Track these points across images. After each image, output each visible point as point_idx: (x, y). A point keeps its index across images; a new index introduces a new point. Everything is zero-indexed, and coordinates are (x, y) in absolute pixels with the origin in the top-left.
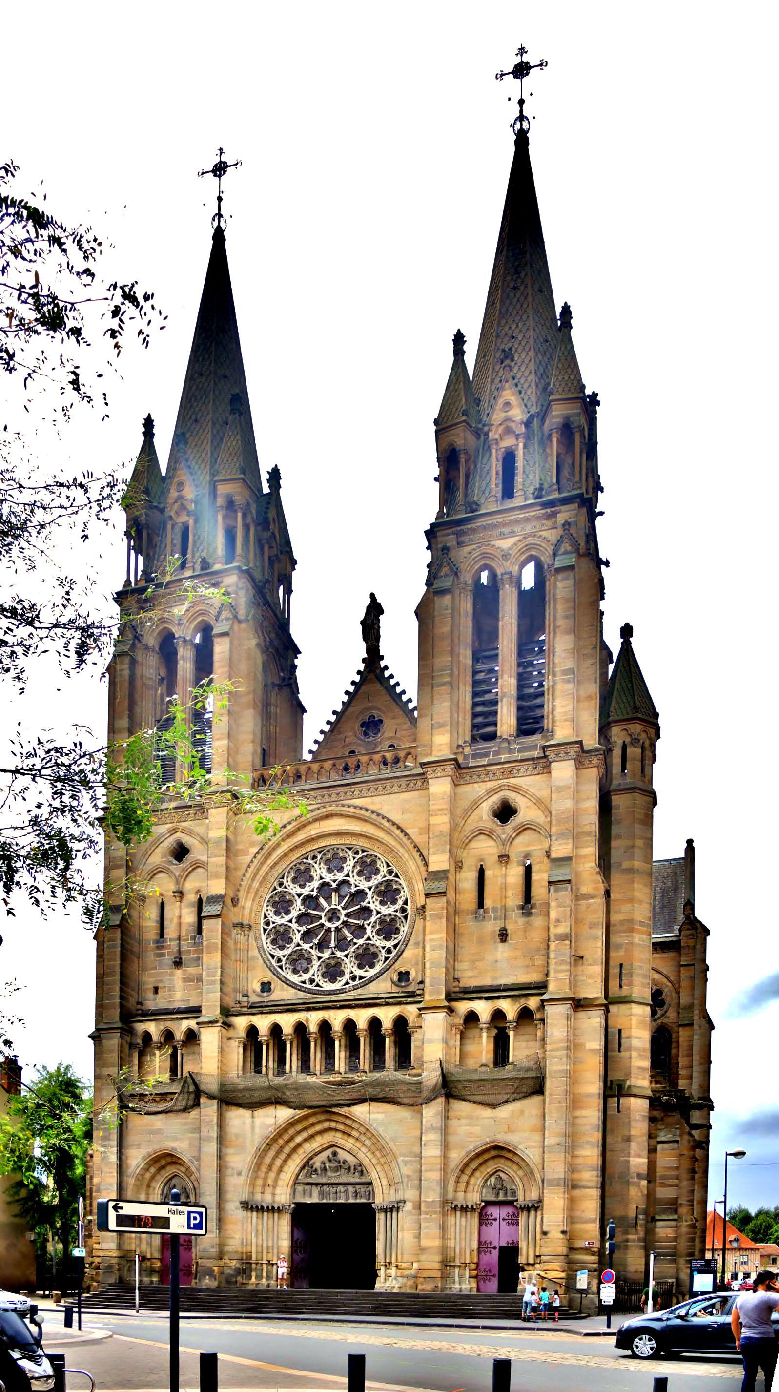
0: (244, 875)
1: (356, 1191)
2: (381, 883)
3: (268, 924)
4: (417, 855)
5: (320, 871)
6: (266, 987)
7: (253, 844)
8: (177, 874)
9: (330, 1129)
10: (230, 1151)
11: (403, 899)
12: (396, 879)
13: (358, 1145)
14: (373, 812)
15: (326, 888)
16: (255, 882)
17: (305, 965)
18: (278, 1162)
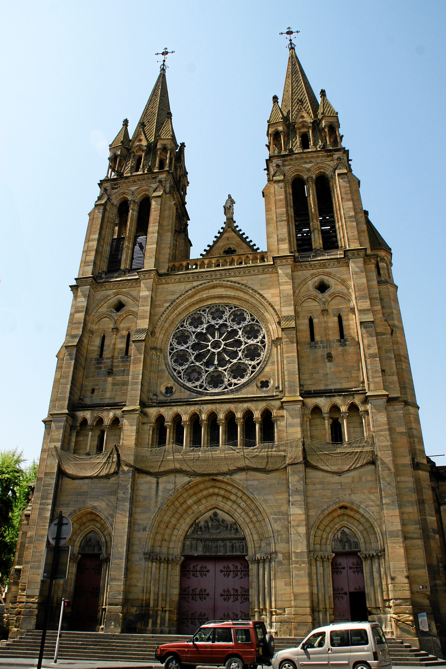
0: (160, 319)
1: (233, 546)
2: (247, 326)
3: (172, 349)
4: (271, 309)
5: (207, 318)
6: (169, 390)
7: (166, 301)
8: (116, 318)
9: (214, 494)
10: (139, 510)
11: (262, 335)
12: (257, 323)
13: (235, 506)
14: (242, 285)
15: (211, 328)
16: (166, 324)
17: (196, 375)
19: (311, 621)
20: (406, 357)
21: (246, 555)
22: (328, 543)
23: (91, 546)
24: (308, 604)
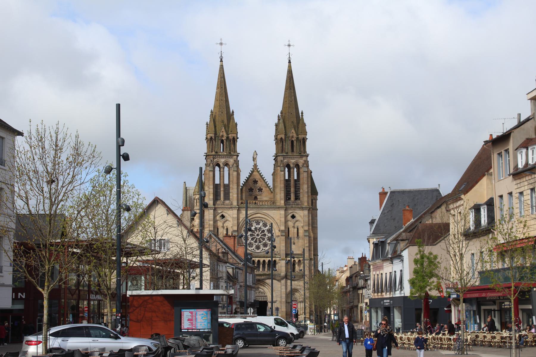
5: (254, 224)
20: (317, 239)
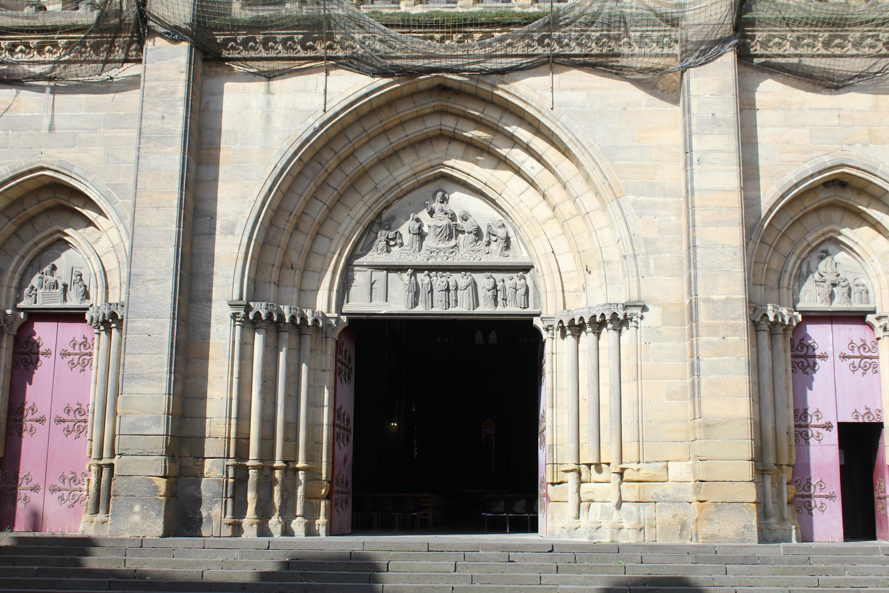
1: (495, 286)
18: (318, 210)
19: (754, 499)
21: (538, 315)
22: (785, 283)
23: (56, 285)
24: (746, 449)
